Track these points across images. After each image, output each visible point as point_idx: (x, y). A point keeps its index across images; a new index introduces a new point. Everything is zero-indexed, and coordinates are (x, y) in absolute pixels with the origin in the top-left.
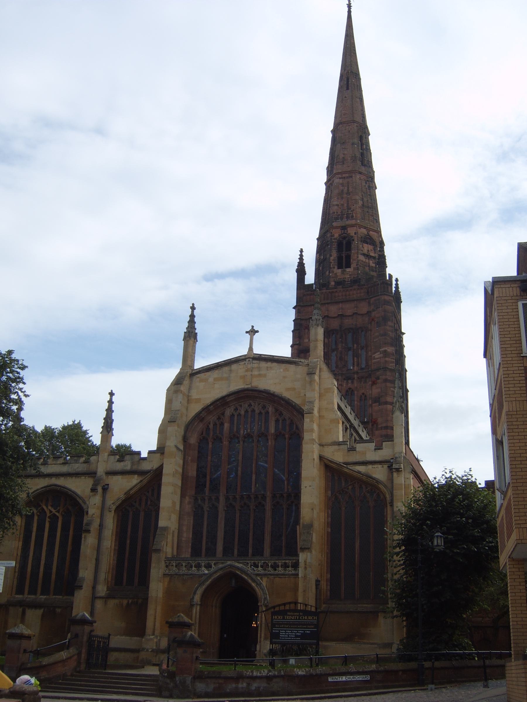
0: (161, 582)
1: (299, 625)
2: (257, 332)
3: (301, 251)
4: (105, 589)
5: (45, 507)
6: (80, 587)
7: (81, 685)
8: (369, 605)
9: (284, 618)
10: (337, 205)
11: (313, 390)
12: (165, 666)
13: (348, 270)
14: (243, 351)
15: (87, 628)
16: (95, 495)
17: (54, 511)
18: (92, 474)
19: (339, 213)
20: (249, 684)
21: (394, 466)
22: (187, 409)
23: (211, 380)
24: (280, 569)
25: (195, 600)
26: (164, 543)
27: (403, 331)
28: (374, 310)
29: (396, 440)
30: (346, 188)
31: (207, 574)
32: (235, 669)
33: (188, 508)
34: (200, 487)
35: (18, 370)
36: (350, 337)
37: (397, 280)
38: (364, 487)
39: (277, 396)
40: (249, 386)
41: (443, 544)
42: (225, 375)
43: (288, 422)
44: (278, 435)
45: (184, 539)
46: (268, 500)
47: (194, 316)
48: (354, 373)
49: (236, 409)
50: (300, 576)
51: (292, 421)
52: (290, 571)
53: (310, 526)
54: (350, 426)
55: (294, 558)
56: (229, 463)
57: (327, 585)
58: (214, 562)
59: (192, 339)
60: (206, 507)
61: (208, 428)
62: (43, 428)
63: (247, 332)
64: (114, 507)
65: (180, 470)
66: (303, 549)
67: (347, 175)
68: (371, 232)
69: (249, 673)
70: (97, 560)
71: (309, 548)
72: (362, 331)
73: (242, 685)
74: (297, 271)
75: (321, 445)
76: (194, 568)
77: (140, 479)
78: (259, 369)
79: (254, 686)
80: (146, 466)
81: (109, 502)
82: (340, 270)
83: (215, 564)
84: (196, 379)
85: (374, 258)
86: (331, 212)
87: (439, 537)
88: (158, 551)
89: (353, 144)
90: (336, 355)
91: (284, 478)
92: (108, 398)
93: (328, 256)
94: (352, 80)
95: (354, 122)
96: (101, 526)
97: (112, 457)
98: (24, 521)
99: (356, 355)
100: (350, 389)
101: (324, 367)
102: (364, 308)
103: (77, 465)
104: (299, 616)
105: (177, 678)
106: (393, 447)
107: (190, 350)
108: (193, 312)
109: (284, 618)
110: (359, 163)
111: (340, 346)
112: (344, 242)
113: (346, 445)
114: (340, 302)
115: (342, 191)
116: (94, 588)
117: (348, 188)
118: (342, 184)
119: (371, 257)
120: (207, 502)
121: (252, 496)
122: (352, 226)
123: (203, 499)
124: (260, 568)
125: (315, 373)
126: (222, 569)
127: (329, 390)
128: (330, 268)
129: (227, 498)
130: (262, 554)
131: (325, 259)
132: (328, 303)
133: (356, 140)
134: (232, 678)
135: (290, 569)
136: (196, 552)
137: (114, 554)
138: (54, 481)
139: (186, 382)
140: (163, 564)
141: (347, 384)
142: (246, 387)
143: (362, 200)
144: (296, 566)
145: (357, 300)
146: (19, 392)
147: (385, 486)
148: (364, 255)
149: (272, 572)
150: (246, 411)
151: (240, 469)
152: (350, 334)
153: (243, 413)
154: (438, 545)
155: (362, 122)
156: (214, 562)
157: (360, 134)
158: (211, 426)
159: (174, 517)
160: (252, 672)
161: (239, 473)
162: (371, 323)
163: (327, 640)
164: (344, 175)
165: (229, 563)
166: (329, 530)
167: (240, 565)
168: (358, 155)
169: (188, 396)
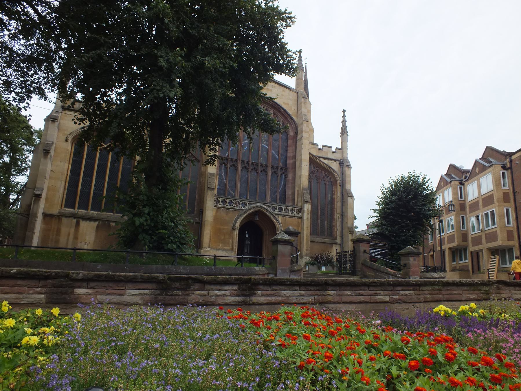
25: (236, 226)
38: (323, 172)
52: (295, 214)
58: (248, 202)
124: (277, 210)
126: (254, 208)
129: (243, 162)
149: (285, 214)
156: (248, 202)
165: (258, 204)
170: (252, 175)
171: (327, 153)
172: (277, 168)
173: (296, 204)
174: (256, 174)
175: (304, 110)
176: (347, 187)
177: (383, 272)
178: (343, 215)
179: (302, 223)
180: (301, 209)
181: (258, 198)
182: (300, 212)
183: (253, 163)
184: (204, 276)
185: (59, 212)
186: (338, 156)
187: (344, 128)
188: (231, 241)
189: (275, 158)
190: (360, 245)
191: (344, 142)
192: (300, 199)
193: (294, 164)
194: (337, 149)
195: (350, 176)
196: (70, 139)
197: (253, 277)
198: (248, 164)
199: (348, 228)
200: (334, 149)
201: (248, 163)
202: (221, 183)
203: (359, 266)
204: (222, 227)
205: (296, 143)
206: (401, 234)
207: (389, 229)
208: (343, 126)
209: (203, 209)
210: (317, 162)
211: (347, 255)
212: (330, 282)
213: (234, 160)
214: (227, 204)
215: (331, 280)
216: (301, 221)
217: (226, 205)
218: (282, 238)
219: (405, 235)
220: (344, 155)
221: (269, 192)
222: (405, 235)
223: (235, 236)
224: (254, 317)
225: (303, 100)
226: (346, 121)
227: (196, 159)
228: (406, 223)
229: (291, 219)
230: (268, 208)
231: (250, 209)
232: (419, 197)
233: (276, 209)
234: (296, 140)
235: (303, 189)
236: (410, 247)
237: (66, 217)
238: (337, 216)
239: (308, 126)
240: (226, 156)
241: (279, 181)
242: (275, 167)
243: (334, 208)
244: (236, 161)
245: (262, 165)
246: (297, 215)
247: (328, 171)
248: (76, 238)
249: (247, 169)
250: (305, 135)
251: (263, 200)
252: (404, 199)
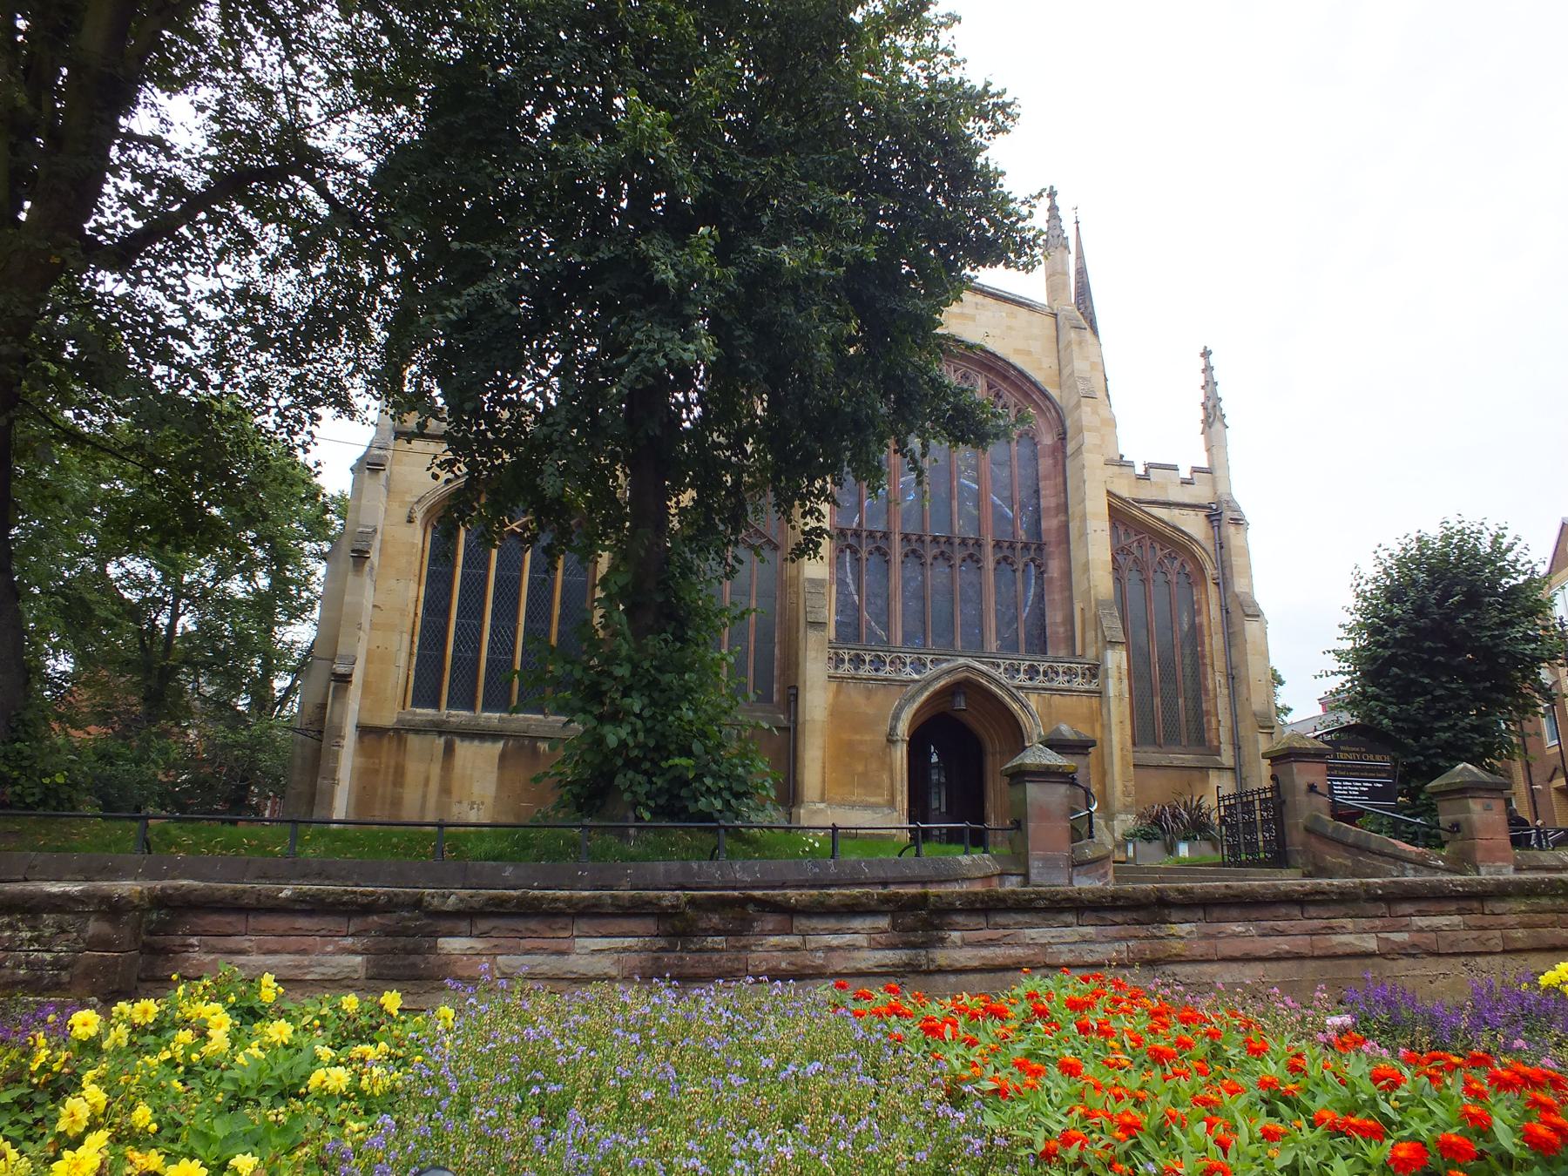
38: (1158, 547)
46: (989, 549)
52: (1078, 683)
124: (1022, 676)
126: (949, 672)
129: (906, 538)
149: (1047, 685)
165: (961, 661)
167: (983, 668)
170: (937, 575)
171: (1164, 487)
172: (1012, 546)
173: (1078, 651)
174: (948, 570)
175: (1080, 365)
176: (1239, 586)
177: (1382, 854)
178: (1233, 677)
179: (1104, 711)
180: (1097, 667)
181: (958, 643)
182: (1095, 676)
183: (935, 540)
184: (790, 892)
186: (1200, 493)
187: (1210, 404)
188: (885, 777)
189: (1004, 516)
190: (1295, 770)
191: (1214, 450)
192: (1090, 635)
193: (1065, 527)
194: (1195, 470)
195: (1246, 553)
197: (933, 890)
198: (923, 542)
199: (1255, 715)
200: (1185, 473)
201: (920, 539)
202: (844, 605)
203: (1296, 838)
204: (858, 737)
205: (1064, 466)
206: (1438, 725)
207: (1392, 709)
208: (1207, 398)
209: (797, 688)
210: (1134, 518)
211: (1253, 802)
212: (1173, 894)
213: (878, 535)
214: (867, 667)
215: (1177, 890)
216: (1101, 705)
217: (865, 671)
218: (1037, 762)
219: (1451, 728)
220: (1221, 489)
221: (991, 623)
222: (1451, 728)
223: (899, 763)
224: (935, 1010)
225: (1073, 335)
226: (1216, 384)
227: (769, 542)
228: (1446, 689)
229: (1068, 698)
230: (993, 672)
231: (938, 678)
232: (1487, 599)
233: (1018, 671)
234: (1065, 457)
235: (1098, 603)
236: (1465, 768)
238: (1216, 680)
239: (1095, 412)
240: (854, 526)
241: (1020, 586)
242: (1006, 544)
243: (1203, 657)
244: (886, 536)
245: (964, 542)
246: (1087, 687)
247: (1174, 544)
249: (920, 557)
250: (1090, 439)
251: (976, 647)
252: (1435, 609)
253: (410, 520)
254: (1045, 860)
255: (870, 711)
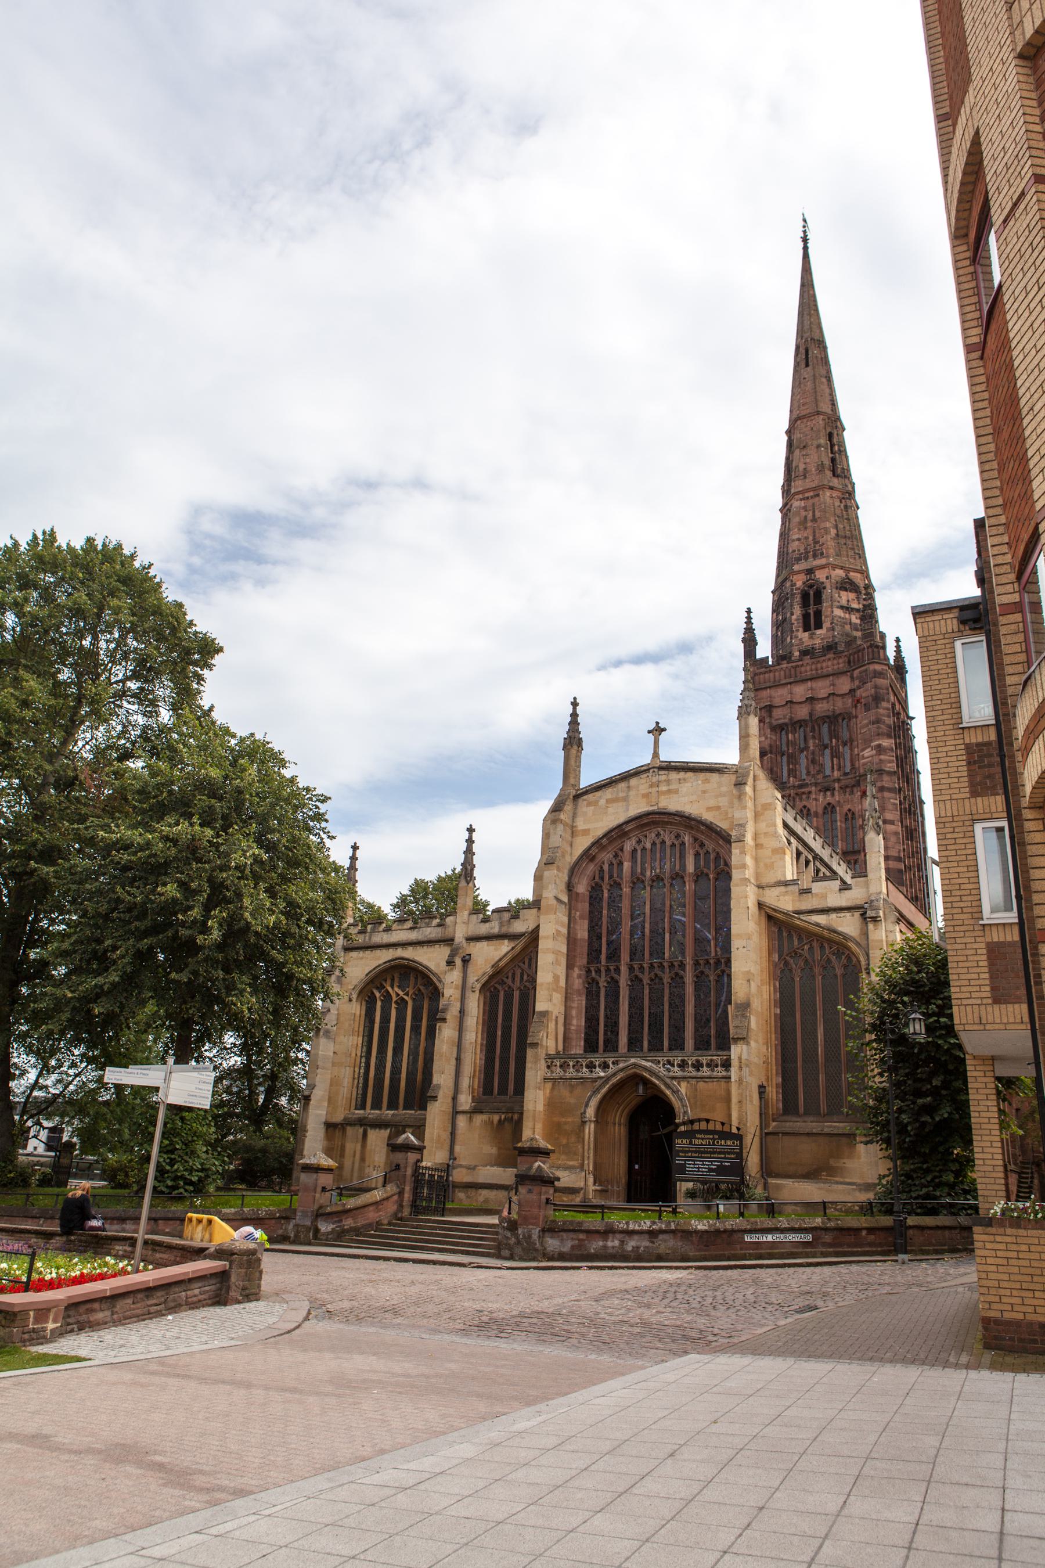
0: (540, 1089)
1: (714, 1153)
2: (664, 730)
3: (749, 611)
4: (470, 1101)
5: (390, 989)
6: (434, 1098)
7: (397, 1239)
8: (841, 1125)
9: (691, 1143)
10: (799, 540)
11: (745, 807)
12: (505, 1213)
13: (818, 632)
14: (646, 759)
15: (412, 1157)
16: (452, 970)
17: (401, 993)
18: (448, 941)
19: (802, 551)
20: (622, 1242)
21: (869, 914)
22: (571, 845)
23: (602, 802)
24: (705, 1069)
25: (587, 1115)
26: (543, 1034)
27: (911, 714)
28: (859, 688)
29: (871, 875)
30: (811, 513)
31: (602, 1078)
32: (603, 1219)
33: (578, 983)
34: (594, 954)
35: (318, 803)
36: (825, 728)
37: (898, 640)
39: (694, 820)
40: (655, 808)
41: (923, 1031)
42: (621, 795)
43: (712, 856)
44: (700, 876)
45: (573, 1028)
46: (688, 968)
47: (577, 715)
48: (834, 781)
49: (639, 842)
50: (733, 1080)
51: (718, 853)
52: (720, 1072)
53: (746, 1006)
54: (814, 858)
55: (725, 1053)
56: (632, 920)
57: (777, 1092)
59: (575, 747)
60: (602, 982)
61: (602, 870)
62: (413, 882)
63: (649, 732)
64: (478, 986)
65: (565, 931)
66: (737, 1040)
67: (811, 494)
68: (852, 574)
69: (622, 1226)
70: (458, 1060)
71: (743, 1039)
72: (843, 719)
73: (613, 1243)
74: (744, 640)
75: (760, 887)
76: (585, 1069)
77: (512, 945)
78: (668, 782)
79: (631, 1244)
80: (519, 927)
81: (472, 979)
82: (807, 634)
83: (613, 1063)
84: (582, 802)
85: (858, 610)
86: (790, 551)
87: (917, 1021)
88: (535, 1045)
89: (819, 446)
90: (807, 758)
91: (710, 937)
92: (466, 835)
93: (788, 615)
94: (815, 352)
95: (818, 413)
96: (462, 1012)
97: (475, 916)
98: (364, 1008)
99: (836, 754)
100: (829, 804)
101: (761, 774)
102: (844, 685)
103: (429, 930)
104: (714, 1139)
105: (520, 1231)
106: (867, 885)
107: (572, 762)
108: (575, 709)
109: (691, 1143)
110: (829, 473)
111: (811, 743)
112: (812, 593)
113: (796, 887)
114: (807, 680)
115: (806, 517)
116: (454, 1099)
117: (814, 512)
118: (805, 508)
119: (853, 609)
120: (603, 974)
121: (665, 964)
122: (822, 567)
123: (598, 971)
125: (745, 784)
127: (769, 807)
128: (792, 632)
129: (631, 968)
130: (682, 1048)
131: (784, 620)
132: (790, 683)
133: (822, 441)
134: (597, 1232)
135: (719, 1069)
136: (591, 1046)
137: (481, 1050)
138: (400, 952)
139: (568, 807)
140: (543, 1064)
141: (825, 796)
142: (651, 809)
143: (836, 527)
144: (727, 1065)
145: (833, 675)
146: (321, 833)
147: (858, 944)
148: (842, 607)
149: (694, 1074)
150: (654, 844)
151: (647, 925)
152: (826, 725)
153: (648, 846)
154: (915, 1033)
155: (830, 412)
157: (829, 430)
158: (606, 867)
159: (558, 998)
160: (627, 1223)
161: (647, 931)
162: (856, 707)
163: (778, 1176)
164: (806, 495)
165: (633, 1060)
166: (778, 1011)
167: (648, 1064)
168: (827, 462)
169: (572, 827)
171: (824, 897)
172: (707, 962)
185: (345, 1119)
196: (354, 996)
201: (641, 967)
217: (571, 1072)
229: (710, 1084)
237: (351, 1125)
248: (363, 1159)
249: (641, 980)
253: (350, 1000)
254: (302, 1212)
255: (572, 1101)
